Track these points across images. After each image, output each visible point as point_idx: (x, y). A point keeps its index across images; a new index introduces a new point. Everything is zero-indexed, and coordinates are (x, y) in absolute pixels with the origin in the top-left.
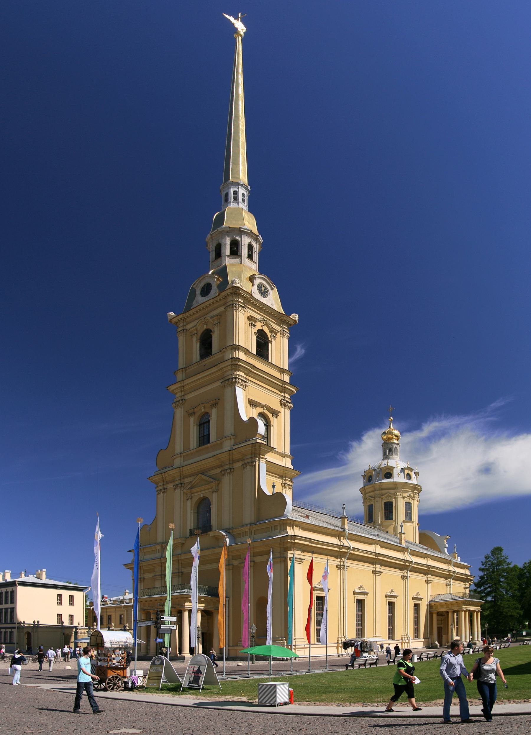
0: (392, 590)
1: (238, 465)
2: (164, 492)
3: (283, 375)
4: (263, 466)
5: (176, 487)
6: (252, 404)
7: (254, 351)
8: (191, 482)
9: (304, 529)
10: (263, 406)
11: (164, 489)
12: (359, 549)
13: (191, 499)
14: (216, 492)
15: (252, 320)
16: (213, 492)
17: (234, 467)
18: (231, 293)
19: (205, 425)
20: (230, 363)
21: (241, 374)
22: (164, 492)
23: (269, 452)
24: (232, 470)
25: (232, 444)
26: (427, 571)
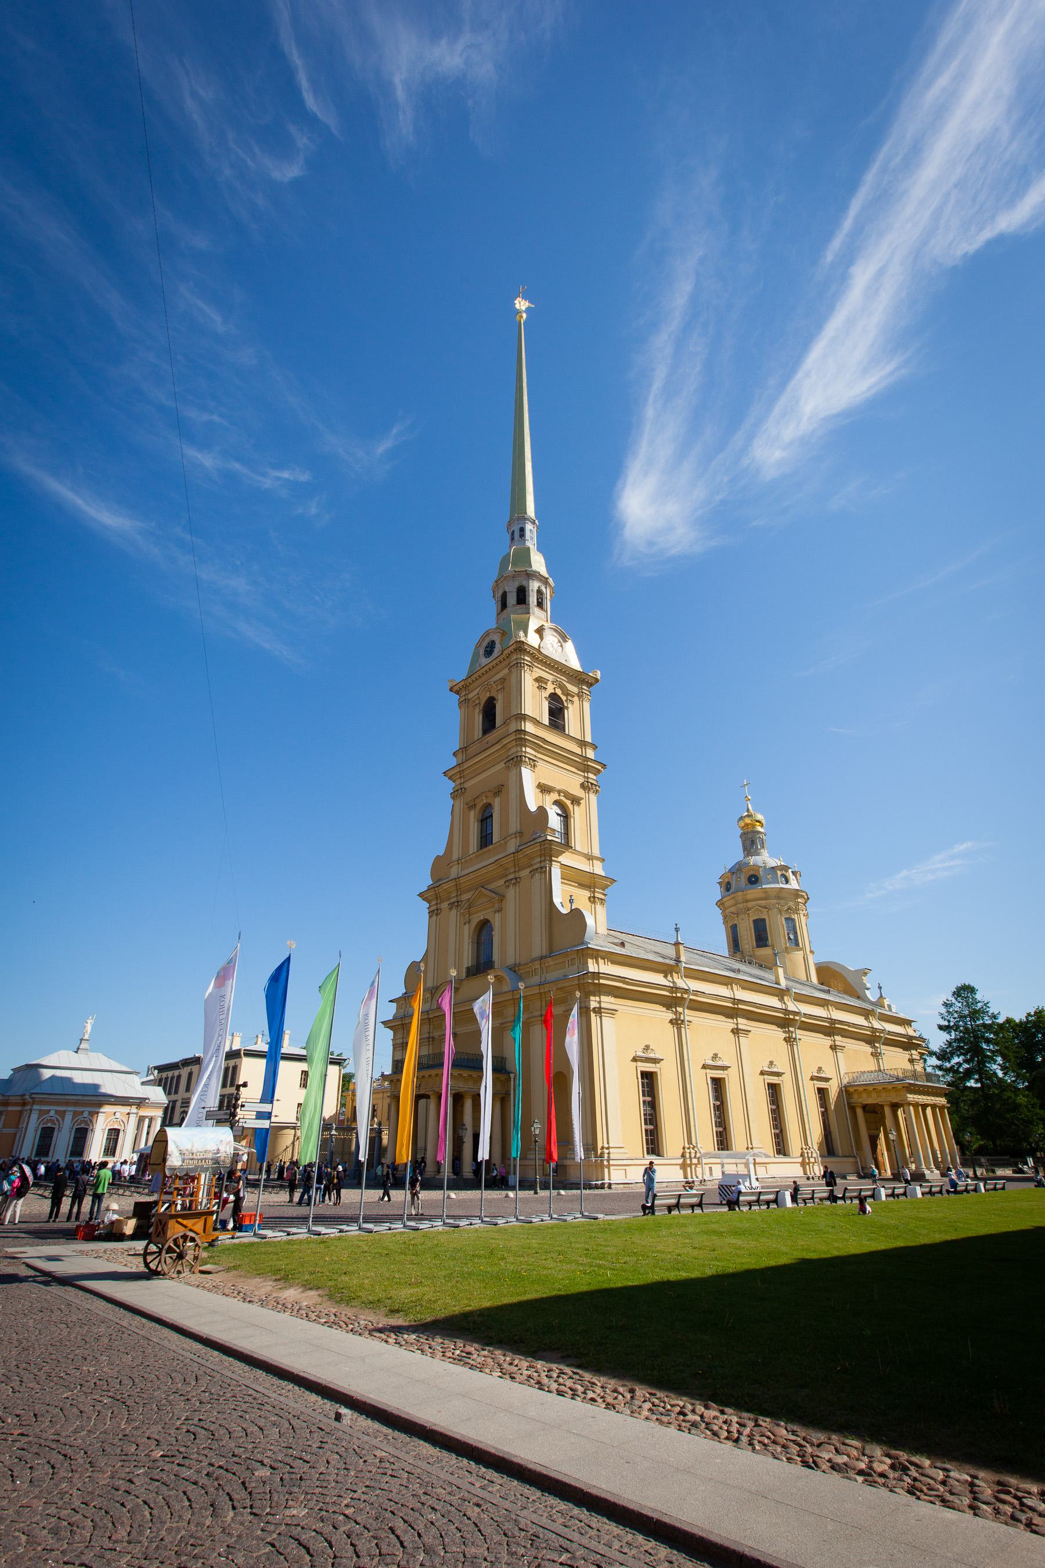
0: (771, 1063)
1: (525, 873)
2: (437, 914)
3: (585, 749)
4: (556, 872)
5: (451, 906)
6: (544, 789)
7: (546, 721)
8: (469, 899)
9: (614, 962)
10: (559, 792)
11: (437, 910)
12: (704, 993)
13: (469, 922)
14: (499, 911)
15: (542, 682)
16: (495, 912)
17: (521, 876)
18: (515, 650)
19: (488, 820)
20: (514, 738)
21: (528, 750)
22: (437, 914)
23: (564, 852)
24: (518, 880)
25: (518, 844)
26: (830, 1029)
